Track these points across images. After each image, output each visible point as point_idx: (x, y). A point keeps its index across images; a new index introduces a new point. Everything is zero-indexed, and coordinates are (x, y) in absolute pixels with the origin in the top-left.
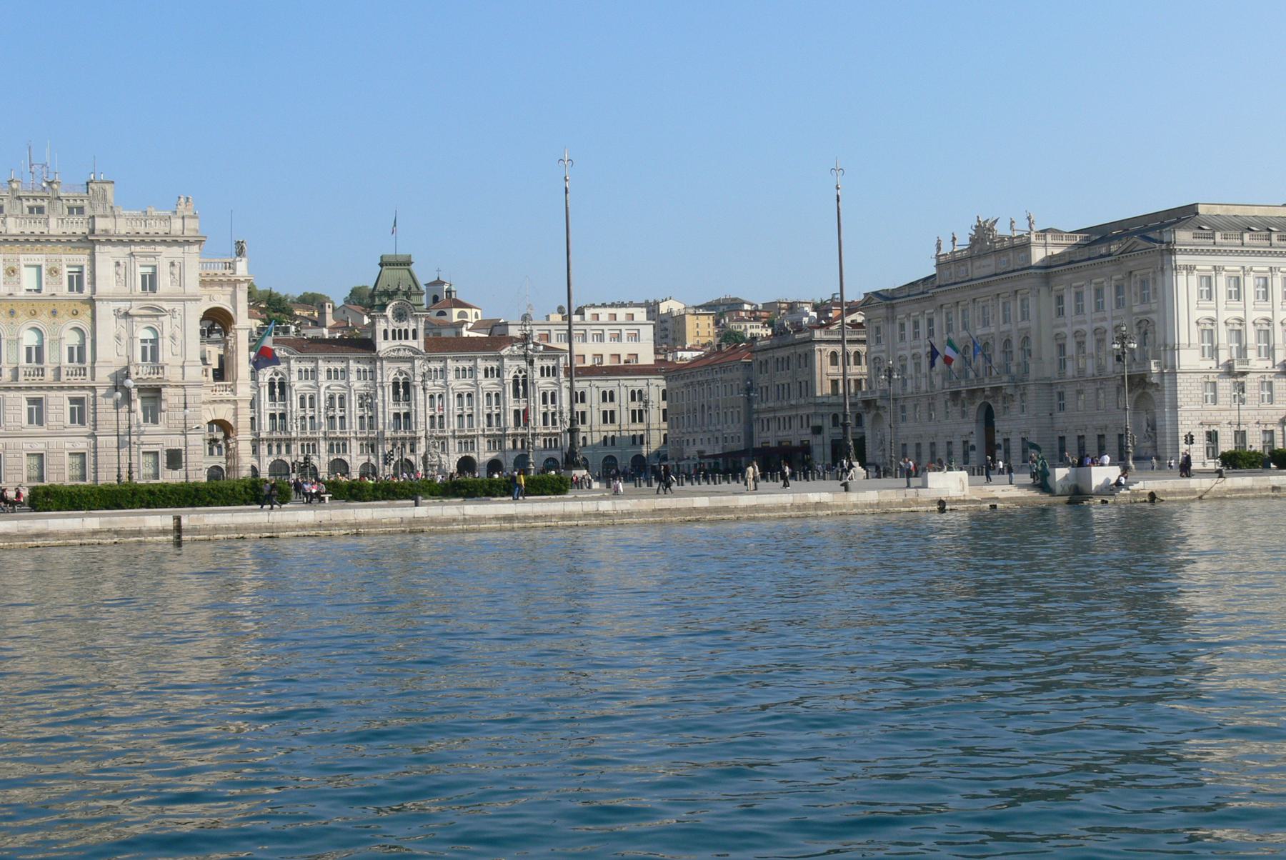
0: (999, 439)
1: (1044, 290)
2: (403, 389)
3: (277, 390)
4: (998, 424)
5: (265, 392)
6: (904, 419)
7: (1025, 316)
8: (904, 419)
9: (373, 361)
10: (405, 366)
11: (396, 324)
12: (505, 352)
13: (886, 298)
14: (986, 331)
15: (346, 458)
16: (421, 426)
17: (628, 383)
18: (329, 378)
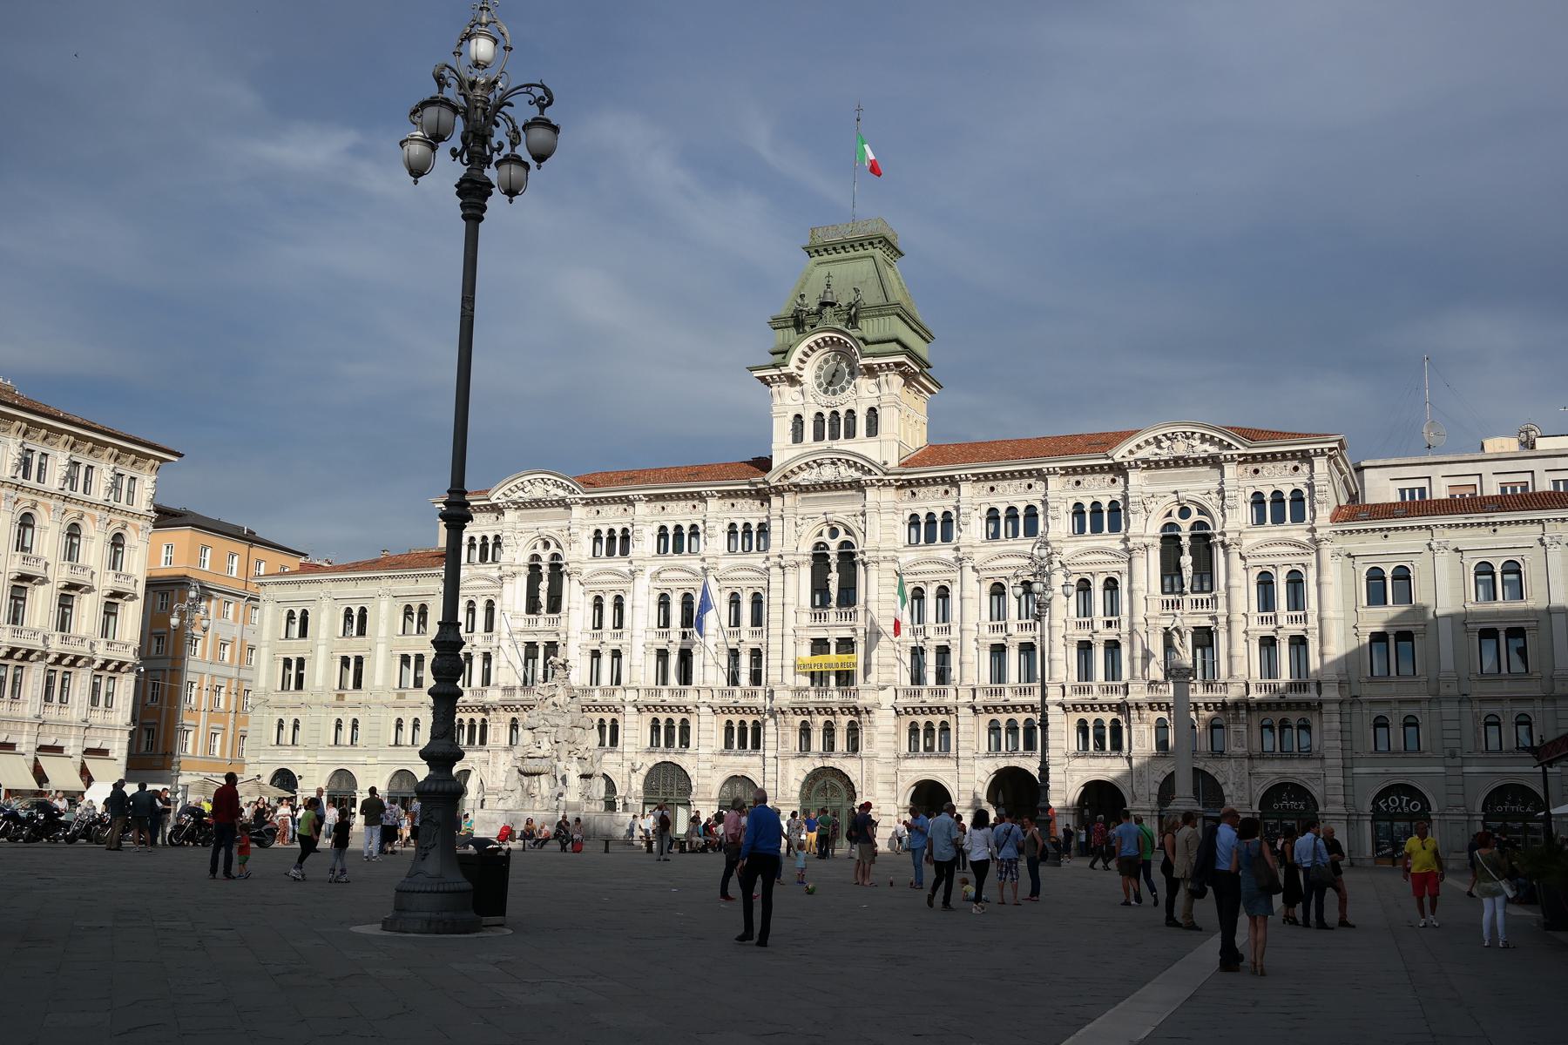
2: (836, 574)
3: (544, 585)
10: (841, 509)
11: (823, 399)
12: (1120, 454)
15: (685, 762)
16: (885, 679)
18: (662, 550)
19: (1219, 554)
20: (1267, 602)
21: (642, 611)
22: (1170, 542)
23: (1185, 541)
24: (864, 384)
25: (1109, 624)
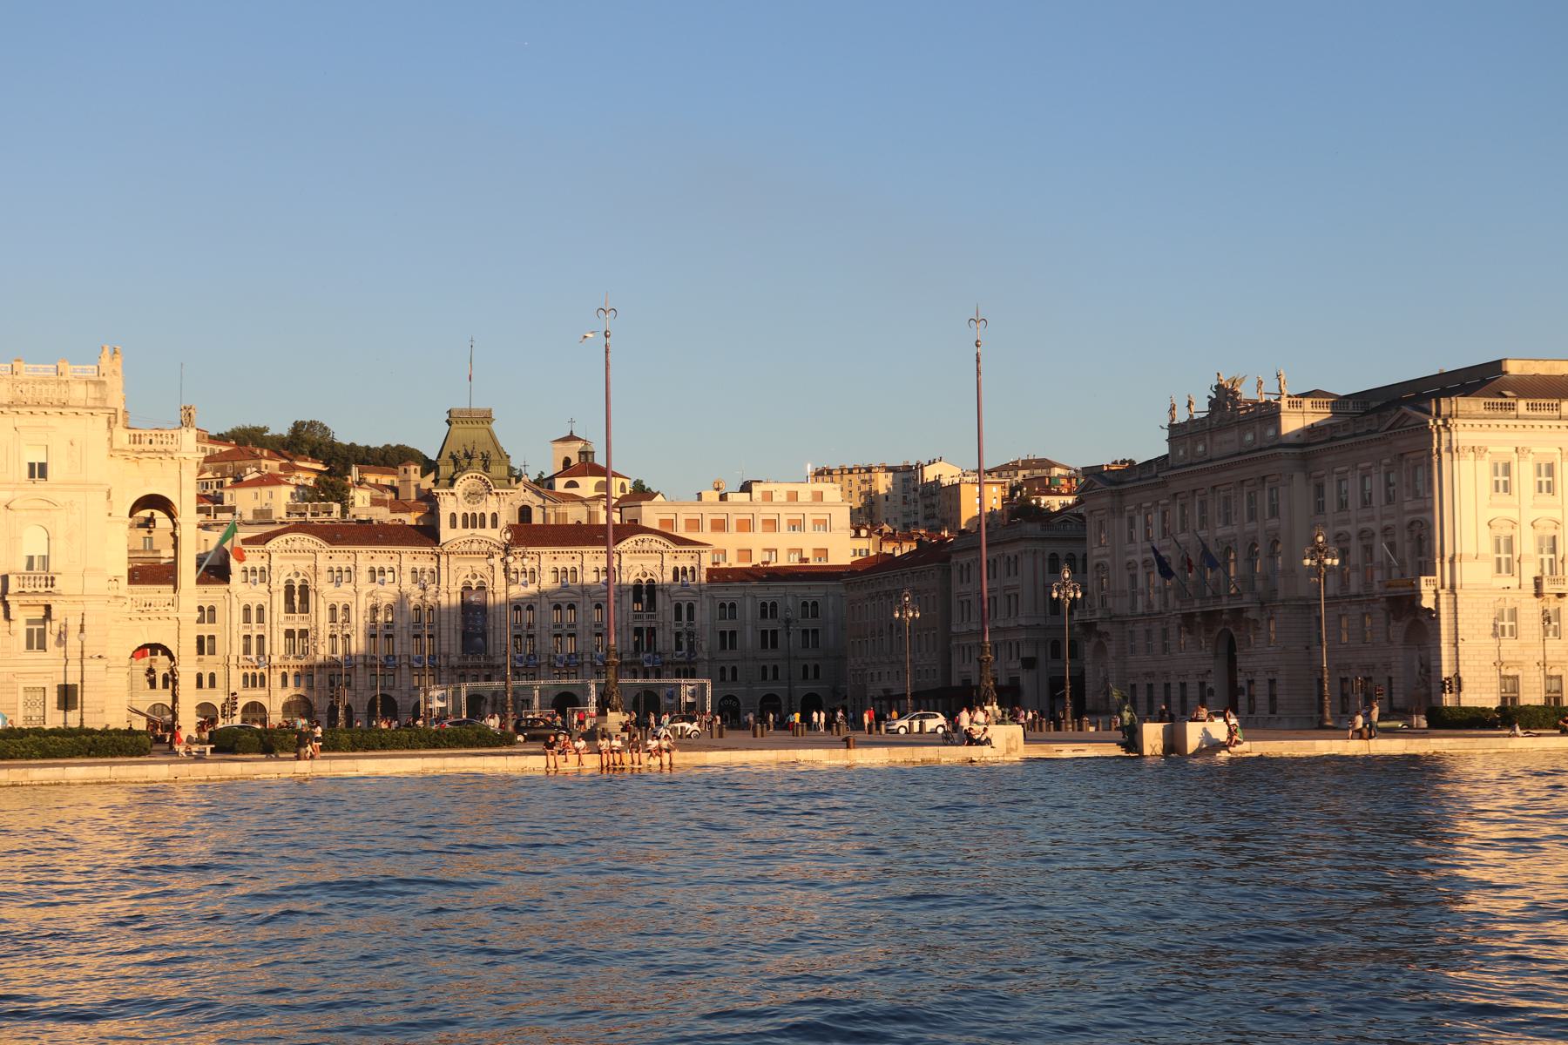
0: (1241, 681)
1: (1299, 477)
3: (297, 597)
4: (1241, 662)
5: (280, 599)
6: (1133, 650)
7: (1274, 512)
8: (1133, 650)
13: (1112, 483)
14: (1228, 530)
17: (798, 592)
20: (678, 617)
24: (492, 499)
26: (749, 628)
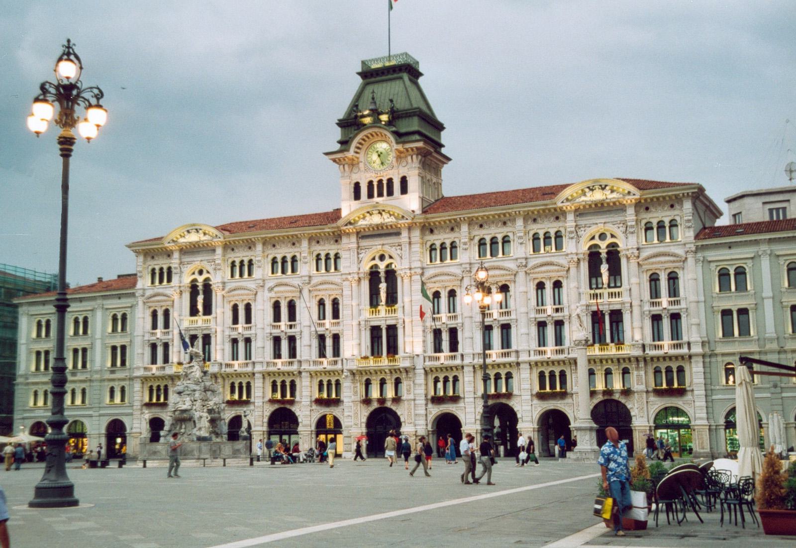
2: (382, 284)
9: (337, 237)
19: (623, 262)
20: (655, 293)
21: (262, 313)
22: (594, 257)
23: (604, 256)
25: (557, 310)
26: (768, 305)
